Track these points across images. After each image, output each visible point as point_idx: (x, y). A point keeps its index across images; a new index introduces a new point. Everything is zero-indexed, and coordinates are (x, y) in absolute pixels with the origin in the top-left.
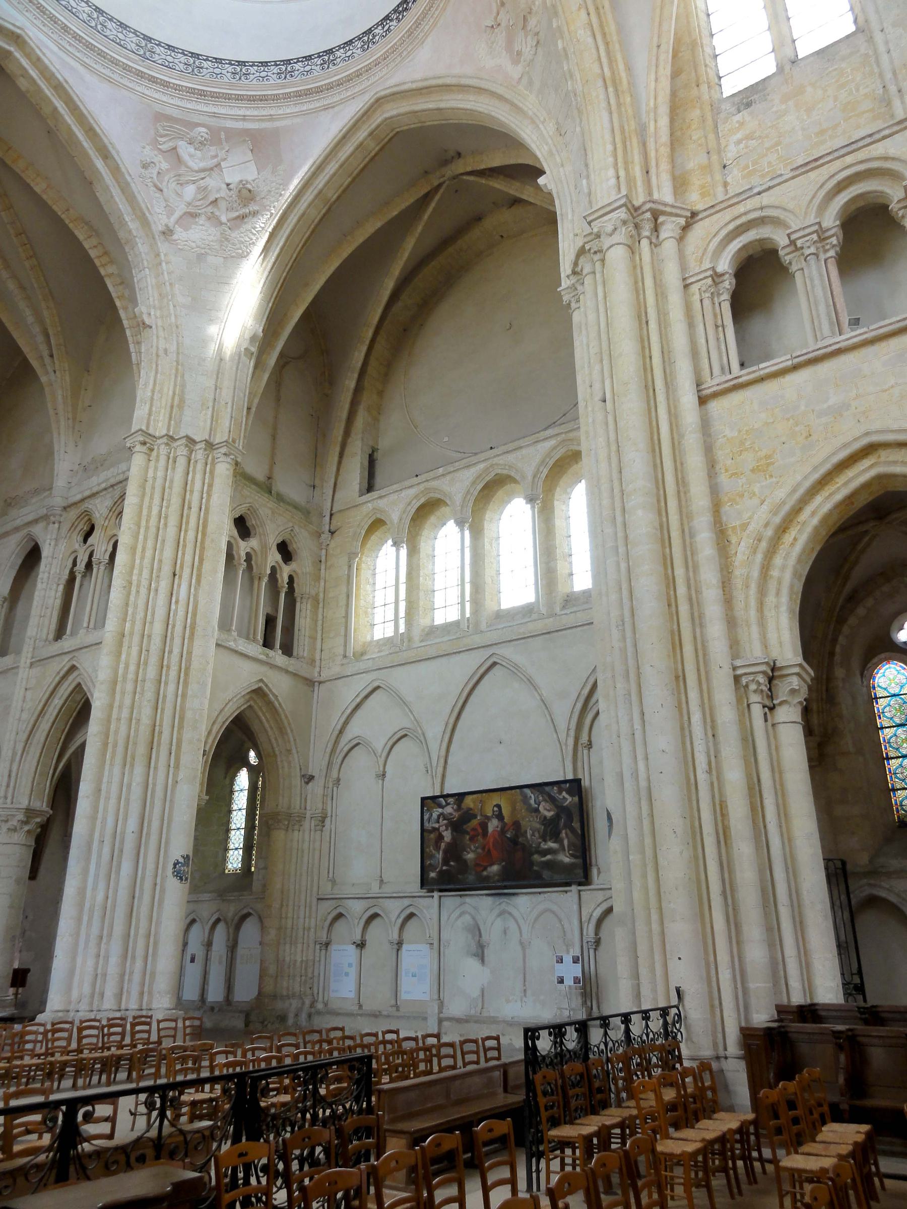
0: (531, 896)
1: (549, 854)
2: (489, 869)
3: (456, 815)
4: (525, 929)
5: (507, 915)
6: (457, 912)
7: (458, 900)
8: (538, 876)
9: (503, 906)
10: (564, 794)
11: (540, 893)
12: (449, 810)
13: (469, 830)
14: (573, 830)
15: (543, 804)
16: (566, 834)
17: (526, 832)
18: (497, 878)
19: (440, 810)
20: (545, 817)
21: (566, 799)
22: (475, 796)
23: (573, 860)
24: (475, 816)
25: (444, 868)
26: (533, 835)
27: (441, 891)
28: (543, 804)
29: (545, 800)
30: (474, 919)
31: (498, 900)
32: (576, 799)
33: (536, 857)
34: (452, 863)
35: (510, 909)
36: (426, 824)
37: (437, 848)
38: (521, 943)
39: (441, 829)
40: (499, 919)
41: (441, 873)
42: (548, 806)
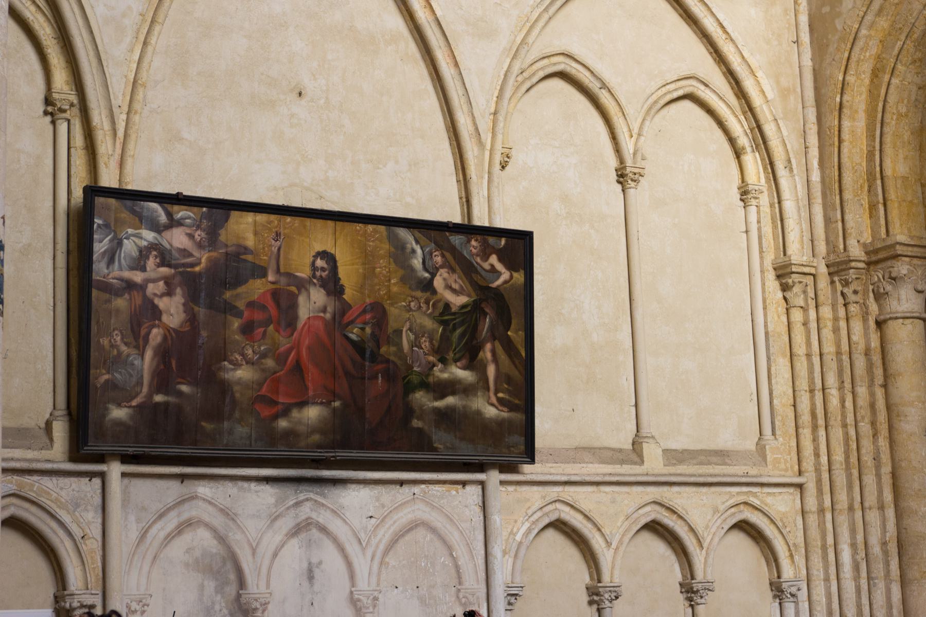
0: (379, 489)
1: (453, 393)
2: (295, 413)
3: (204, 258)
4: (362, 565)
5: (315, 533)
6: (171, 522)
7: (173, 489)
8: (422, 442)
9: (306, 511)
10: (494, 259)
11: (401, 483)
12: (178, 239)
13: (241, 304)
14: (509, 346)
15: (443, 272)
16: (494, 352)
17: (398, 332)
18: (316, 438)
19: (149, 236)
20: (447, 306)
21: (499, 274)
22: (262, 218)
23: (505, 415)
24: (261, 272)
25: (159, 398)
26: (416, 344)
27: (126, 459)
28: (443, 272)
29: (446, 265)
30: (222, 539)
31: (292, 495)
32: (519, 277)
33: (420, 398)
34: (184, 388)
35: (323, 517)
36: (100, 268)
37: (138, 340)
38: (354, 602)
39: (151, 288)
40: (294, 542)
41: (148, 412)
42: (456, 281)
